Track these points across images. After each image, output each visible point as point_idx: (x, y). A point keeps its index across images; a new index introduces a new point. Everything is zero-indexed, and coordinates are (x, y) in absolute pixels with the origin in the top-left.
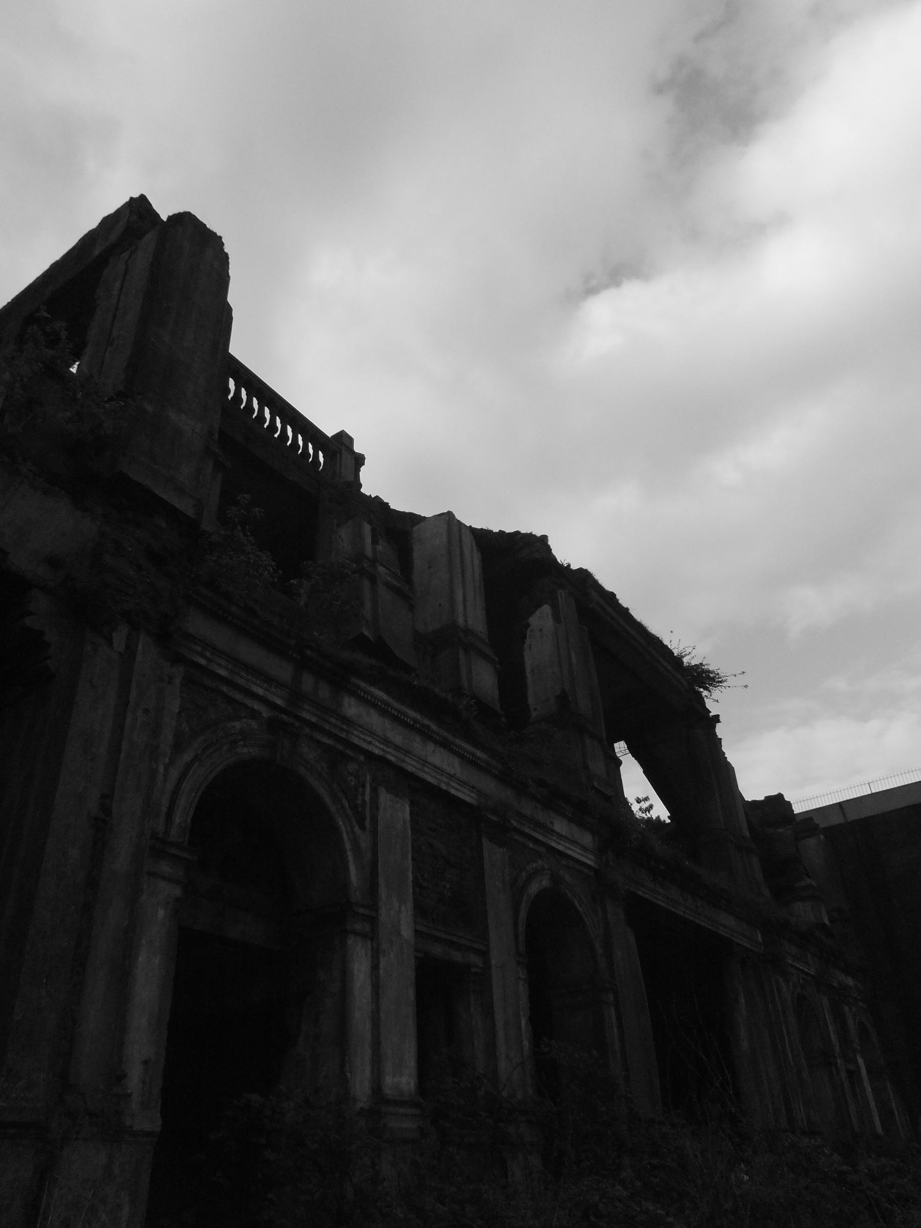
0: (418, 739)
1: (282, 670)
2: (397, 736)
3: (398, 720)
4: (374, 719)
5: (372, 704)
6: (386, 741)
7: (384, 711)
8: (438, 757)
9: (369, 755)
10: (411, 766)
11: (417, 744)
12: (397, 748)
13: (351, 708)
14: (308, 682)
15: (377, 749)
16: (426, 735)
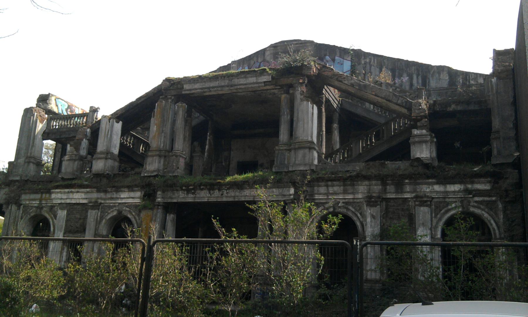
0: (71, 194)
1: (38, 196)
2: (64, 197)
3: (65, 193)
4: (59, 196)
5: (58, 193)
6: (61, 199)
7: (61, 193)
8: (76, 196)
9: (59, 204)
10: (68, 201)
11: (71, 196)
12: (63, 199)
13: (53, 196)
14: (44, 195)
15: (59, 202)
16: (71, 192)
